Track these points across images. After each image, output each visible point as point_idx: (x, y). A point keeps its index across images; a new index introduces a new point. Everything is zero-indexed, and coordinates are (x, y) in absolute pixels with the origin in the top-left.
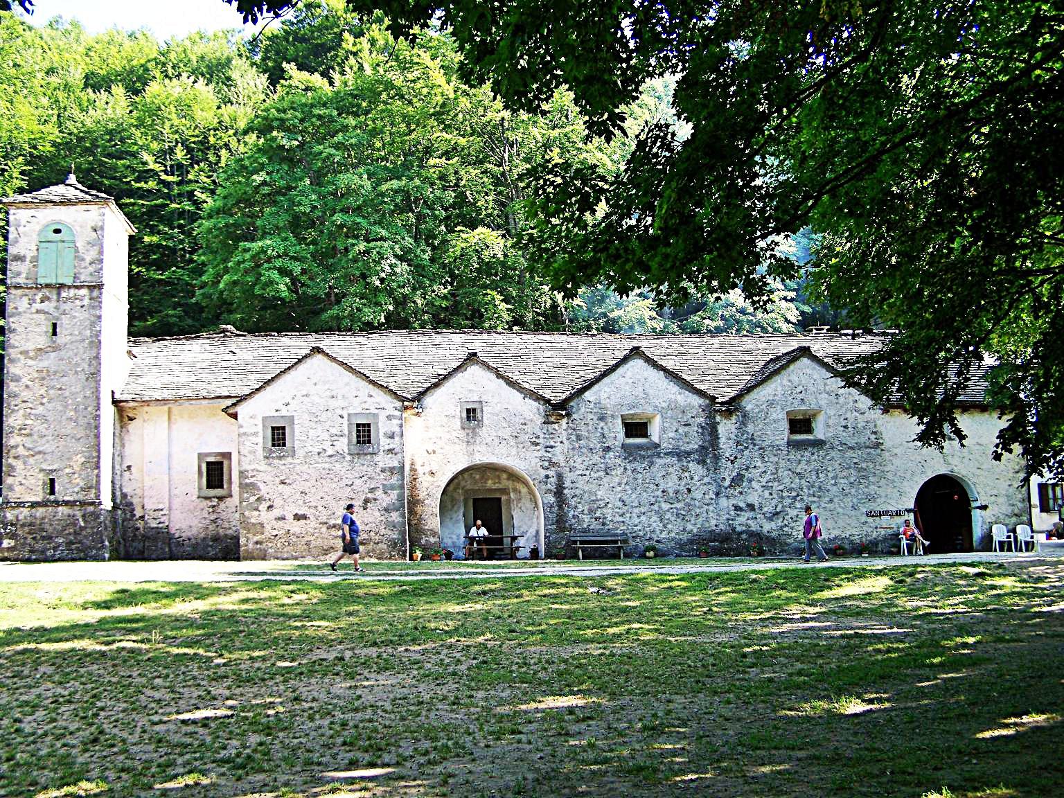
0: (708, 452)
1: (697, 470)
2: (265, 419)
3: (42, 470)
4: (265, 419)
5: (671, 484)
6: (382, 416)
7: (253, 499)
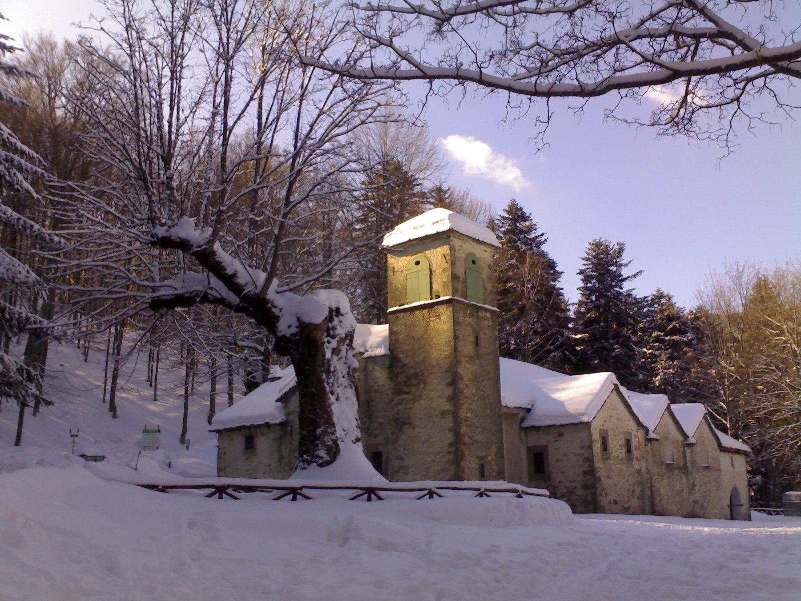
0: (684, 469)
1: (684, 480)
2: (600, 430)
3: (478, 457)
4: (600, 430)
5: (678, 487)
6: (633, 437)
7: (600, 487)
